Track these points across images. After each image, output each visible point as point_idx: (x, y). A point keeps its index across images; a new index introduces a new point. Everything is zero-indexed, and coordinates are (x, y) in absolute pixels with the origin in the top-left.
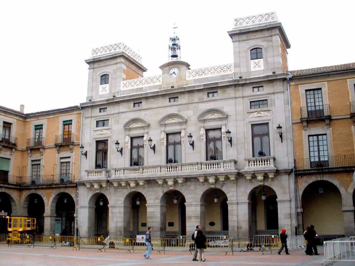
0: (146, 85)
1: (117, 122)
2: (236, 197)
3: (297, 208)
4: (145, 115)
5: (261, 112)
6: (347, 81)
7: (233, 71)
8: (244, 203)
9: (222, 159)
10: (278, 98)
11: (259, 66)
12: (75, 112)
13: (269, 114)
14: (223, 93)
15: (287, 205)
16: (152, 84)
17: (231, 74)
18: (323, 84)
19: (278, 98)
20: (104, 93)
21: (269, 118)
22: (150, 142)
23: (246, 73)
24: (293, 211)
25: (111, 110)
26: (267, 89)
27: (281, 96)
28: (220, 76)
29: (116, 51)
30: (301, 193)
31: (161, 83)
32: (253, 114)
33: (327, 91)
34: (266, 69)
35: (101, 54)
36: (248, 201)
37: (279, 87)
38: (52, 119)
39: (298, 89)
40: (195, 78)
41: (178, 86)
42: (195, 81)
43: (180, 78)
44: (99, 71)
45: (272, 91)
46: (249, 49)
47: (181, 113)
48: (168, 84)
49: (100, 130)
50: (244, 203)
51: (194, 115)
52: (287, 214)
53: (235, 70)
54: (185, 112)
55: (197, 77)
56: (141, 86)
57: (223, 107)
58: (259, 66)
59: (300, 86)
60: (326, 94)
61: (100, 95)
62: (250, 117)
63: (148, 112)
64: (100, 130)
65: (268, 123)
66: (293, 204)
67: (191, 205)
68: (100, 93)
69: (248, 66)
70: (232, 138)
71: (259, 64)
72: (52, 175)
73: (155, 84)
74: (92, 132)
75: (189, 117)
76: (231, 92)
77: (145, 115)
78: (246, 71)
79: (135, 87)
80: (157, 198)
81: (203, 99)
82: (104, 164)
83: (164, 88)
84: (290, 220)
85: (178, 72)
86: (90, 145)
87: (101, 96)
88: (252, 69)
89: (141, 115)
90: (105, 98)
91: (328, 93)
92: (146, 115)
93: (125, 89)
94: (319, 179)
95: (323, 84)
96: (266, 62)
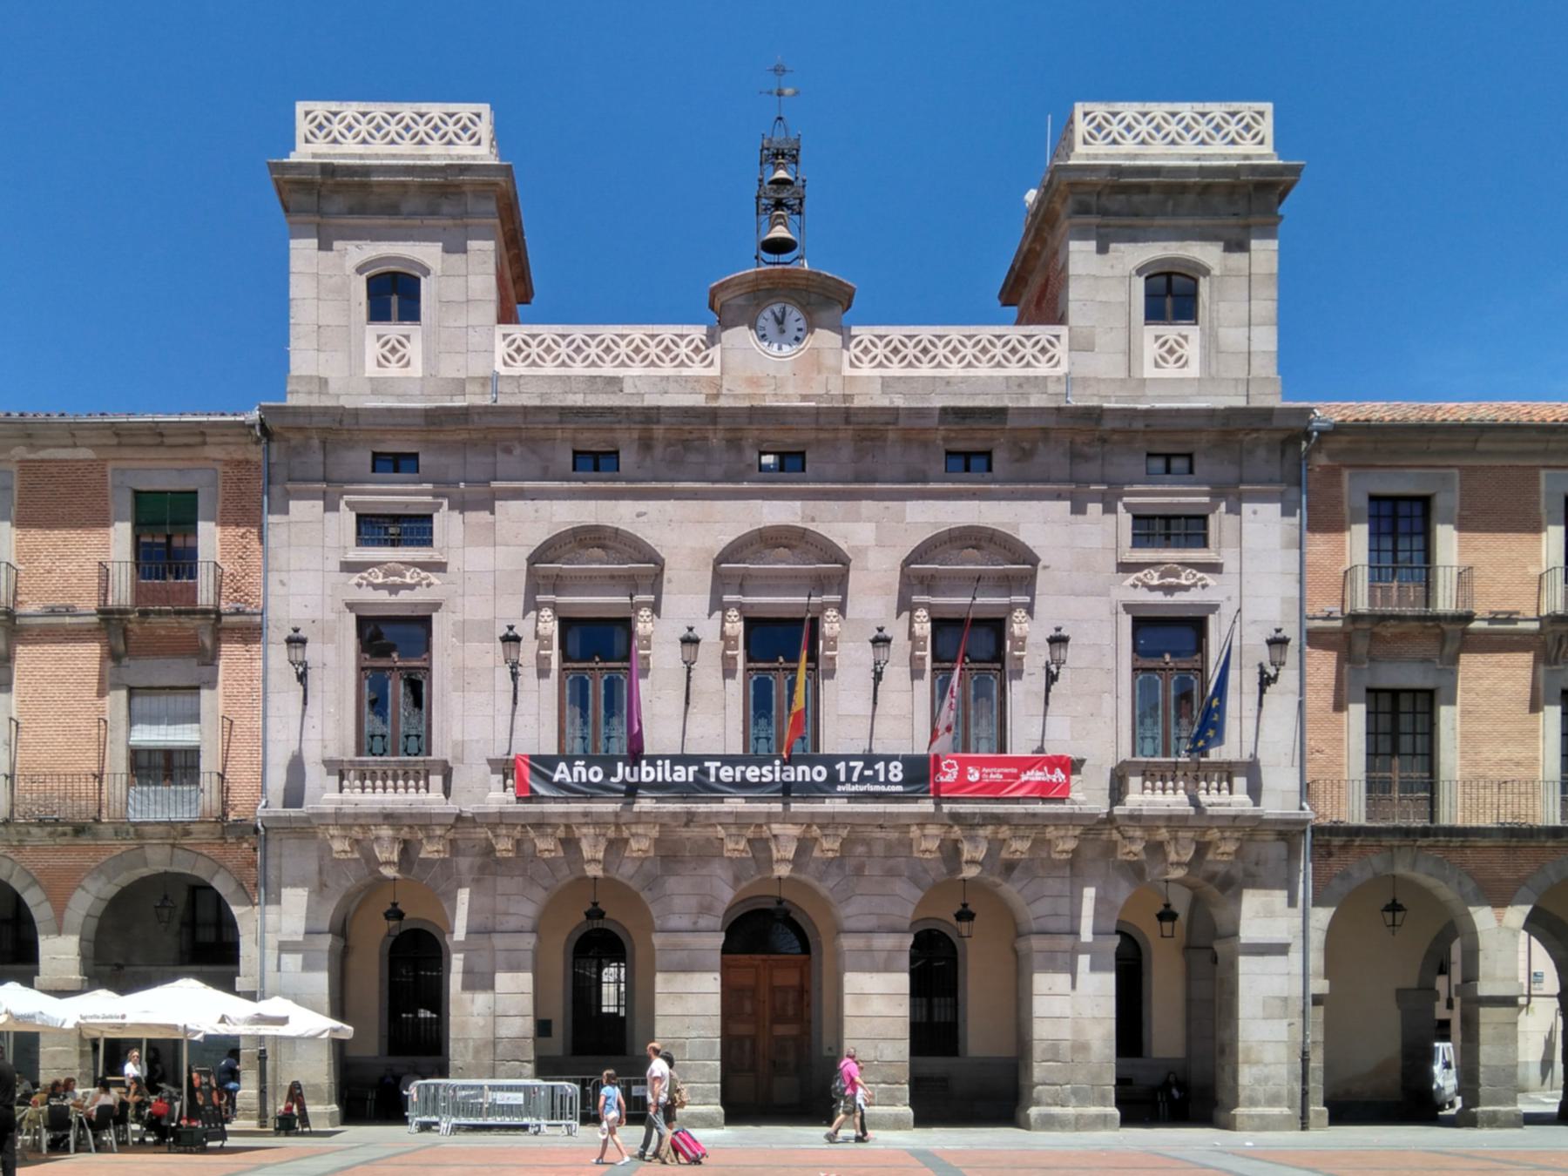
0: (637, 370)
4: (639, 515)
6: (1537, 478)
7: (1062, 370)
14: (1017, 460)
16: (668, 370)
17: (1059, 379)
20: (394, 370)
22: (688, 648)
23: (1122, 380)
28: (1007, 378)
29: (454, 150)
31: (714, 371)
33: (1457, 510)
34: (1208, 380)
35: (361, 149)
39: (1339, 485)
41: (804, 398)
42: (886, 383)
43: (815, 362)
46: (1139, 272)
48: (753, 381)
51: (880, 544)
52: (1275, 998)
53: (1072, 364)
55: (896, 370)
56: (608, 370)
57: (1016, 527)
58: (1181, 357)
61: (371, 379)
68: (371, 370)
69: (1130, 353)
72: (95, 776)
73: (685, 372)
75: (862, 551)
77: (639, 515)
78: (1122, 374)
79: (578, 369)
83: (735, 396)
84: (1285, 1022)
85: (800, 330)
87: (378, 386)
88: (1149, 371)
89: (620, 514)
90: (399, 396)
92: (641, 519)
93: (519, 369)
96: (1211, 347)
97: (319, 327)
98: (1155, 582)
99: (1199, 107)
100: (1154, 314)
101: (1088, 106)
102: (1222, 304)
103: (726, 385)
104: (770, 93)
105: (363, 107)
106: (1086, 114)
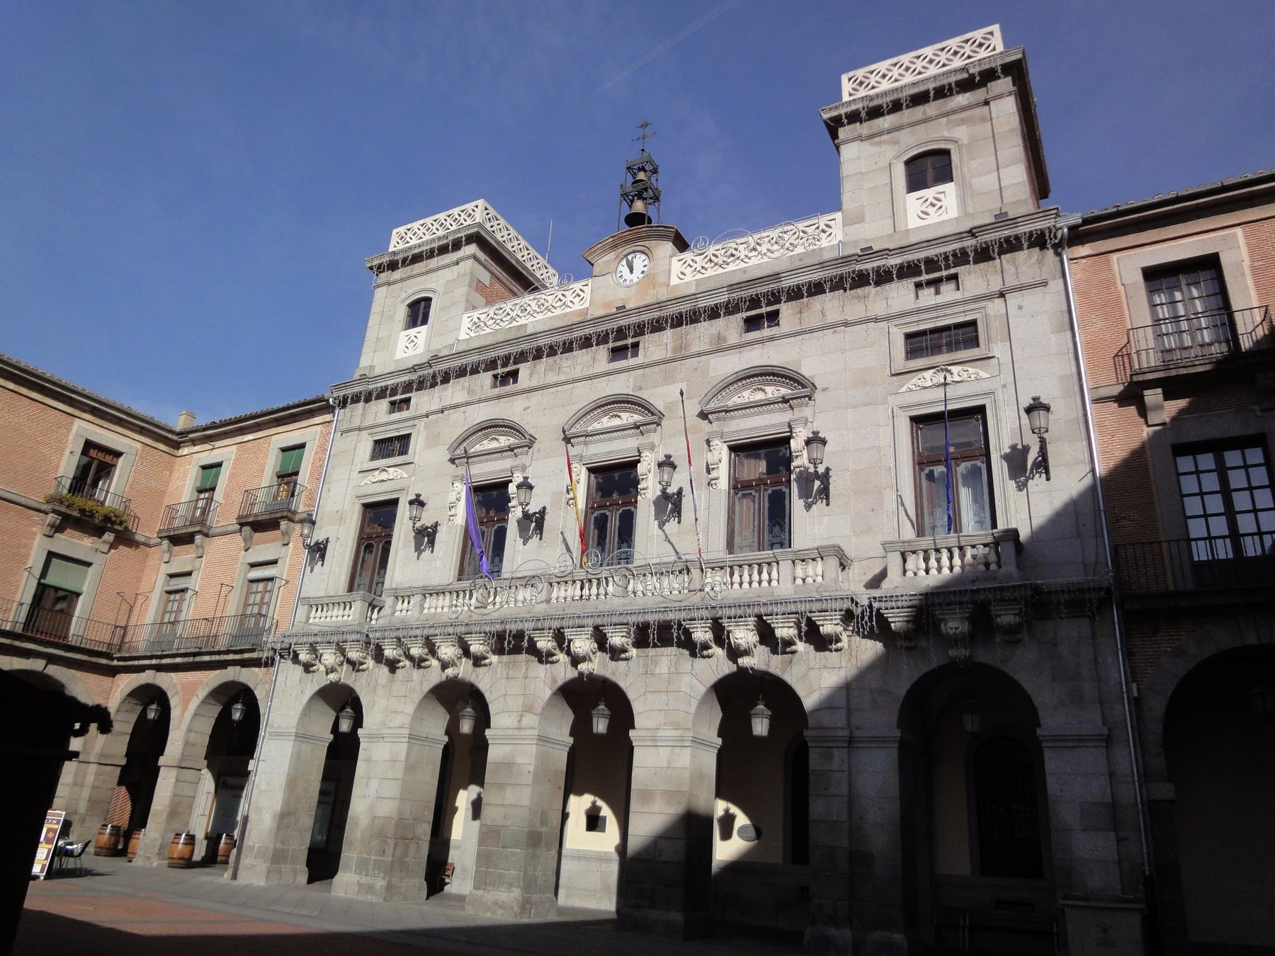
1: (433, 441)
2: (844, 711)
3: (1146, 777)
5: (949, 368)
7: (840, 237)
8: (879, 741)
9: (790, 547)
10: (1020, 308)
11: (941, 207)
12: (318, 420)
13: (984, 375)
15: (1092, 758)
17: (832, 247)
18: (1224, 238)
19: (1020, 308)
21: (985, 387)
23: (889, 236)
24: (1130, 793)
25: (422, 401)
26: (975, 279)
27: (1031, 299)
30: (1157, 706)
31: (587, 305)
32: (920, 376)
36: (898, 733)
37: (1026, 263)
38: (250, 445)
39: (1110, 269)
40: (699, 276)
44: (405, 292)
45: (996, 286)
47: (644, 395)
48: (607, 305)
49: (378, 469)
50: (879, 741)
54: (660, 389)
59: (1115, 256)
60: (1243, 274)
62: (903, 390)
63: (535, 398)
64: (378, 469)
65: (981, 410)
66: (1126, 758)
67: (655, 742)
70: (831, 473)
71: (939, 204)
74: (355, 475)
76: (831, 305)
80: (528, 709)
81: (725, 339)
82: (377, 584)
86: (341, 518)
89: (513, 409)
91: (1253, 269)
94: (1252, 640)
95: (1224, 238)
97: (378, 339)
98: (929, 383)
99: (939, 46)
100: (916, 181)
101: (851, 74)
102: (972, 162)
103: (590, 312)
104: (638, 139)
105: (421, 222)
106: (850, 79)
